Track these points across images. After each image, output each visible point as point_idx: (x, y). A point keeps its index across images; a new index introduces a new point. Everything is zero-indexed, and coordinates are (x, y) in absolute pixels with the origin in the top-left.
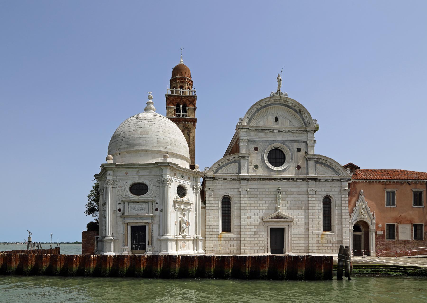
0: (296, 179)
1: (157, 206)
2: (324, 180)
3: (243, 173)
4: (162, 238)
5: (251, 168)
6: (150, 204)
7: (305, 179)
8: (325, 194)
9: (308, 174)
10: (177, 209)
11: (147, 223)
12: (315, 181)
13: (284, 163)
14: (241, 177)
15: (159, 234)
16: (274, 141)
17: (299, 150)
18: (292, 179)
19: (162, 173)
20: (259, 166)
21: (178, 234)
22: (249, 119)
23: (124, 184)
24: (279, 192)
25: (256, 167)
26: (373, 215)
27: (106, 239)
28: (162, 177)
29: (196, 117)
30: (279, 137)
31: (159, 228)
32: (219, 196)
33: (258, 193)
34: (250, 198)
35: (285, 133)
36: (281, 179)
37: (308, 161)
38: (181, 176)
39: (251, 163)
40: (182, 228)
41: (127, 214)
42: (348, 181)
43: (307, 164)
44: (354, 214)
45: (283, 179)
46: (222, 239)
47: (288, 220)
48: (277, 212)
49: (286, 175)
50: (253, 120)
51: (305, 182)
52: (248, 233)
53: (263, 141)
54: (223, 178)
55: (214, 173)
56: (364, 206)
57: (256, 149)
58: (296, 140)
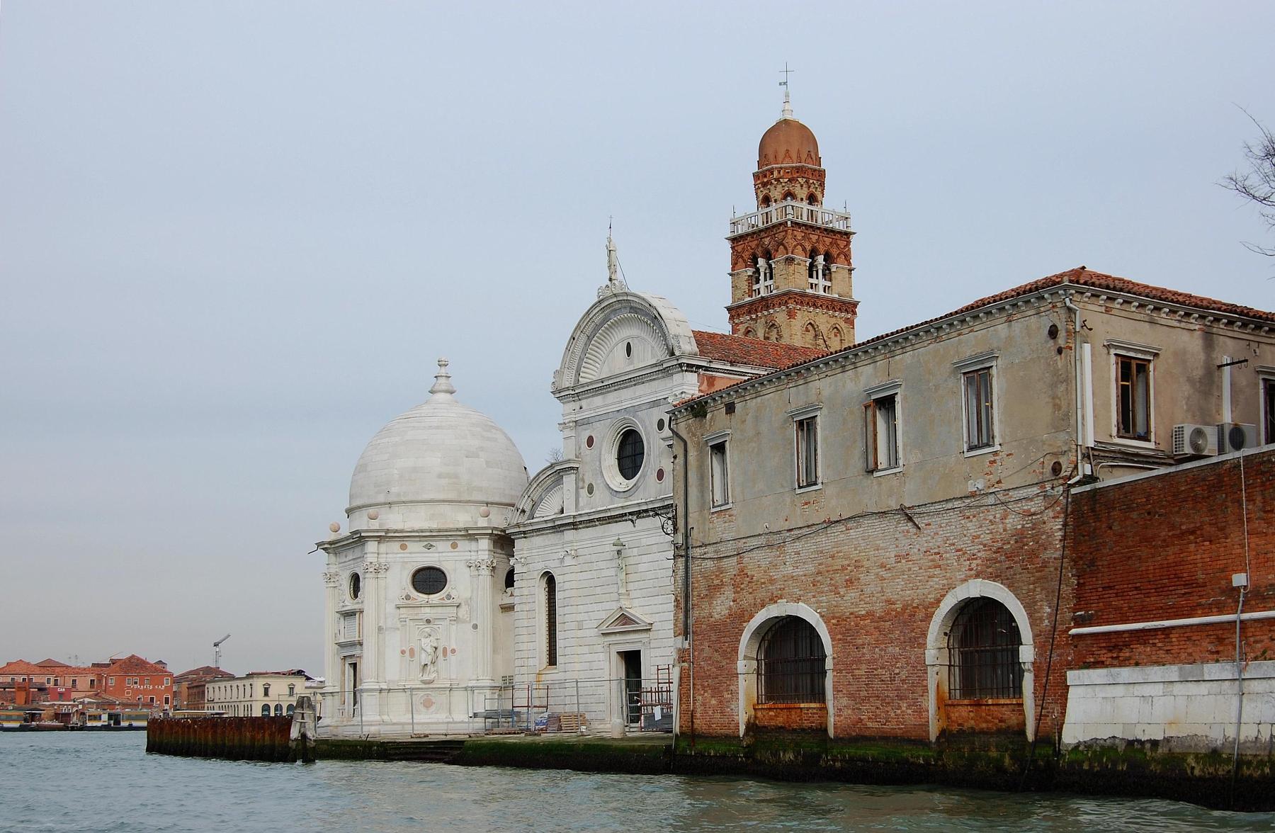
5: (584, 492)
6: (357, 615)
10: (406, 621)
14: (559, 523)
16: (618, 411)
22: (575, 368)
24: (619, 552)
25: (591, 490)
32: (536, 576)
33: (594, 558)
39: (583, 481)
54: (538, 530)
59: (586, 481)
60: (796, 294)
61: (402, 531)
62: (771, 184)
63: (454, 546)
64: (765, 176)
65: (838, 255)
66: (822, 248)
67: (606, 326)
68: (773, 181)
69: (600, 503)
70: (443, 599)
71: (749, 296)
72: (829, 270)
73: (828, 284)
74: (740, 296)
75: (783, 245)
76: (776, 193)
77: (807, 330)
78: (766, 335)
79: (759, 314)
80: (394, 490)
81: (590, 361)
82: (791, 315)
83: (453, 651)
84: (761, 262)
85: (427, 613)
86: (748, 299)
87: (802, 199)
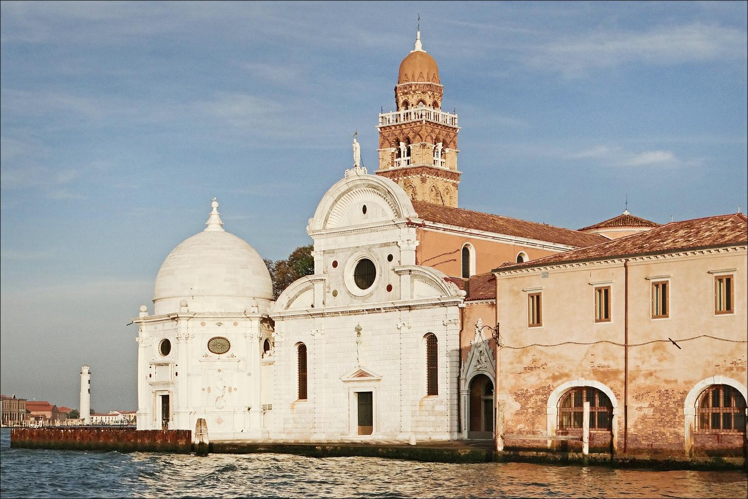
0: (385, 308)
2: (422, 306)
3: (319, 307)
25: (335, 294)
30: (364, 240)
35: (371, 232)
36: (363, 311)
38: (217, 324)
39: (329, 288)
42: (457, 306)
45: (367, 310)
46: (295, 410)
47: (372, 378)
51: (397, 313)
55: (285, 309)
59: (331, 288)
60: (427, 167)
61: (203, 314)
62: (410, 94)
63: (235, 324)
64: (406, 88)
65: (450, 142)
66: (441, 138)
67: (349, 193)
68: (411, 92)
69: (342, 302)
71: (392, 166)
72: (444, 151)
73: (444, 160)
75: (419, 135)
76: (412, 100)
77: (432, 191)
79: (400, 178)
80: (195, 288)
81: (335, 214)
82: (423, 180)
83: (235, 389)
84: (403, 145)
85: (219, 364)
86: (391, 168)
87: (430, 105)
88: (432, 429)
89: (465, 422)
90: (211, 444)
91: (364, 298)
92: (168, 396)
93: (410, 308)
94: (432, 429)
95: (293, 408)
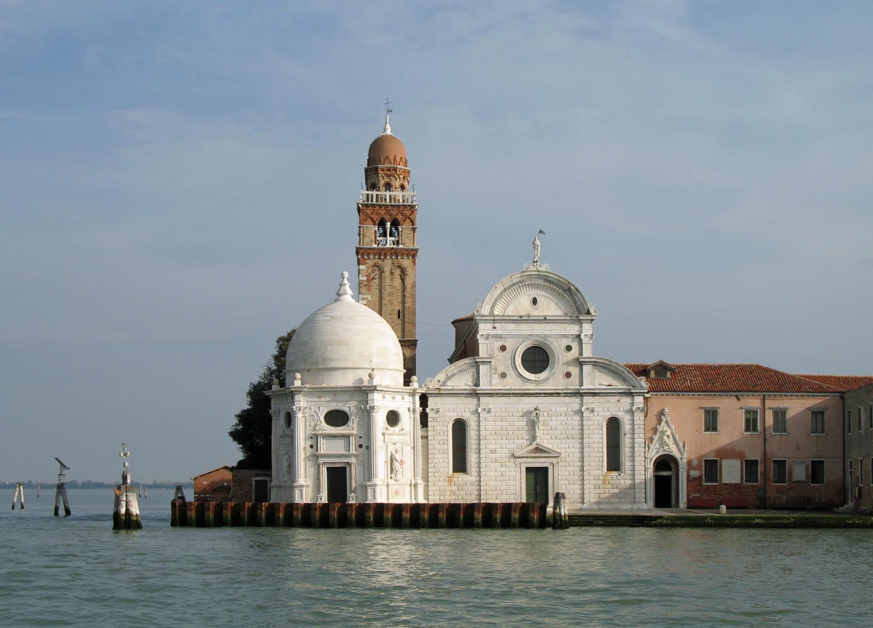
1: (361, 441)
4: (368, 483)
7: (577, 393)
8: (609, 415)
9: (582, 386)
11: (348, 463)
12: (593, 396)
13: (546, 367)
15: (364, 478)
16: (530, 335)
17: (569, 348)
18: (557, 393)
19: (368, 398)
20: (507, 374)
21: (389, 477)
23: (316, 412)
25: (503, 375)
26: (684, 447)
27: (295, 484)
28: (368, 403)
29: (416, 247)
30: (539, 330)
31: (364, 470)
34: (494, 422)
37: (582, 365)
39: (496, 369)
40: (394, 468)
41: (322, 452)
43: (581, 370)
44: (653, 445)
45: (544, 393)
48: (534, 444)
49: (549, 386)
50: (498, 305)
52: (491, 474)
53: (512, 336)
55: (440, 386)
56: (669, 433)
57: (503, 348)
58: (564, 334)
67: (520, 285)
69: (512, 383)
70: (400, 431)
74: (369, 242)
75: (409, 219)
76: (397, 183)
78: (392, 271)
80: (374, 360)
86: (375, 246)
88: (616, 500)
89: (650, 494)
90: (570, 517)
91: (537, 382)
92: (343, 470)
93: (594, 394)
94: (616, 500)
95: (451, 481)
